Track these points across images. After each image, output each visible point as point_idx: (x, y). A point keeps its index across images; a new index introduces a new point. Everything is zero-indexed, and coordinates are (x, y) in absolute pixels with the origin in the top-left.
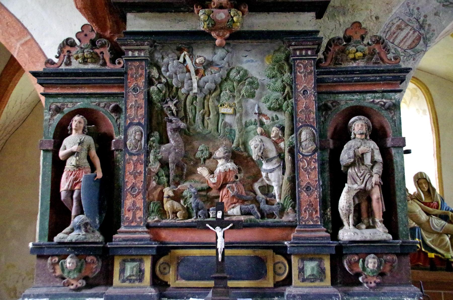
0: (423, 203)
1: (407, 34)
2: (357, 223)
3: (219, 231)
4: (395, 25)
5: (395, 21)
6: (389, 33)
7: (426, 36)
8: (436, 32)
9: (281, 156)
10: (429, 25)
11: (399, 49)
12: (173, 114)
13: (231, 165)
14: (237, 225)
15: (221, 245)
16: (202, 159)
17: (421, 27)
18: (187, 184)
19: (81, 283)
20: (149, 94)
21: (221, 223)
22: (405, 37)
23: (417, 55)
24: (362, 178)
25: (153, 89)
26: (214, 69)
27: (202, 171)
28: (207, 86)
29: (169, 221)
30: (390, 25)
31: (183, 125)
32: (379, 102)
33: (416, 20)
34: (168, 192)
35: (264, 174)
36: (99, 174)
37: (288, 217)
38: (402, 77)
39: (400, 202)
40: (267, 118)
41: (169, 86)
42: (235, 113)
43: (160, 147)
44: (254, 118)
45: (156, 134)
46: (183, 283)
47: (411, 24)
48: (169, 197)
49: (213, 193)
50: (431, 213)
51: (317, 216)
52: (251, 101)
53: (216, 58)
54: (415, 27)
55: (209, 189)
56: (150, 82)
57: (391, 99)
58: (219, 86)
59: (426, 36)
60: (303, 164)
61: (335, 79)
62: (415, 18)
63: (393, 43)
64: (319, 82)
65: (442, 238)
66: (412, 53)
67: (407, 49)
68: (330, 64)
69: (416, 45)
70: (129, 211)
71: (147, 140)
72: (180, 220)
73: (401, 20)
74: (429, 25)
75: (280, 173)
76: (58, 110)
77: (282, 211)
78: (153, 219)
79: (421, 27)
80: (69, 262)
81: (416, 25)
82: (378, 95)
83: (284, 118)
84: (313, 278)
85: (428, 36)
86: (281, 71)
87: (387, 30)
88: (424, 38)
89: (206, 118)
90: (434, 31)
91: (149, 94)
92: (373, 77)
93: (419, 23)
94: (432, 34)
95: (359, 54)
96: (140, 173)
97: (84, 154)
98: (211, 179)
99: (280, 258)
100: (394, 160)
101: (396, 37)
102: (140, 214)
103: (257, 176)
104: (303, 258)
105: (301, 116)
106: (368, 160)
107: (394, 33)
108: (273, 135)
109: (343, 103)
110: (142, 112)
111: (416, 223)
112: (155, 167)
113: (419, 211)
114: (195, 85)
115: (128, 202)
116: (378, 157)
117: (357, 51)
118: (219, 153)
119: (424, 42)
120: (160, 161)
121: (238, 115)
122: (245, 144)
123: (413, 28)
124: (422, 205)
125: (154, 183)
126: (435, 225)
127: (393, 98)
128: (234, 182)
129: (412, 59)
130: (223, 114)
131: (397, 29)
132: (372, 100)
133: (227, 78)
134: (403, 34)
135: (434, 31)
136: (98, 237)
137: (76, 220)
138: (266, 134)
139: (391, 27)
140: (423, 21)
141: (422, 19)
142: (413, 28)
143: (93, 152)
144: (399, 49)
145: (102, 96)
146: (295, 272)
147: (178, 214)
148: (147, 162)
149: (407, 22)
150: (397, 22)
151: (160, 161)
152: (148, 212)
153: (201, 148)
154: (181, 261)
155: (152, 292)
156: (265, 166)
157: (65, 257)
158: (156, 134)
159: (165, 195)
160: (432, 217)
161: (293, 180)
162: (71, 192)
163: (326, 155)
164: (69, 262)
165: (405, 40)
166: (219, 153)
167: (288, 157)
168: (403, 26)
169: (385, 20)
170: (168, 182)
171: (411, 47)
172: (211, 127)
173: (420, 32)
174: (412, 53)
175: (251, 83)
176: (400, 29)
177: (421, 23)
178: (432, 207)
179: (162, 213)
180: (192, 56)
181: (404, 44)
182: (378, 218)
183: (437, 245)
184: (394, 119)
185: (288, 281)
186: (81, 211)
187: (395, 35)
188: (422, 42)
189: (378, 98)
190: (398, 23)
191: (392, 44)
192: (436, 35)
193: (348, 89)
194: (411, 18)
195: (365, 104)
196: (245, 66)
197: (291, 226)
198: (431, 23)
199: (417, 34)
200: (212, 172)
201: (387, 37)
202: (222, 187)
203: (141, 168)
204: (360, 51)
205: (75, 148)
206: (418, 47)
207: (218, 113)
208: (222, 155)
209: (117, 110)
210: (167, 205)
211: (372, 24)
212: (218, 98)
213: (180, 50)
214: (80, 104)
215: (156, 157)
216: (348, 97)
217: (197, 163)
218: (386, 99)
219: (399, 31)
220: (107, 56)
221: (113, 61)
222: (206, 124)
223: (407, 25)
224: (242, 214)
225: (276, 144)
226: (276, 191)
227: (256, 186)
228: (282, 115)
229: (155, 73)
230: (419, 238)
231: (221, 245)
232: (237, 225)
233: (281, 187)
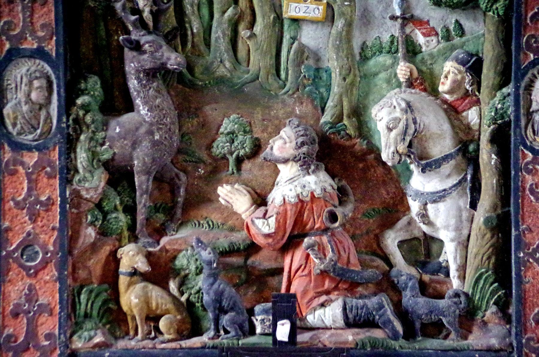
12: (142, 24)
16: (232, 160)
18: (185, 233)
35: (415, 206)
40: (430, 32)
43: (105, 125)
48: (134, 273)
70: (16, 315)
75: (465, 202)
89: (244, 33)
96: (48, 204)
98: (259, 223)
108: (444, 87)
120: (107, 165)
121: (339, 23)
128: (326, 230)
130: (295, 21)
147: (162, 324)
151: (107, 165)
153: (227, 126)
159: (124, 267)
170: (132, 228)
207: (279, 19)
208: (290, 150)
215: (94, 155)
222: (242, 53)
224: (349, 324)
228: (475, 20)
233: (464, 244)
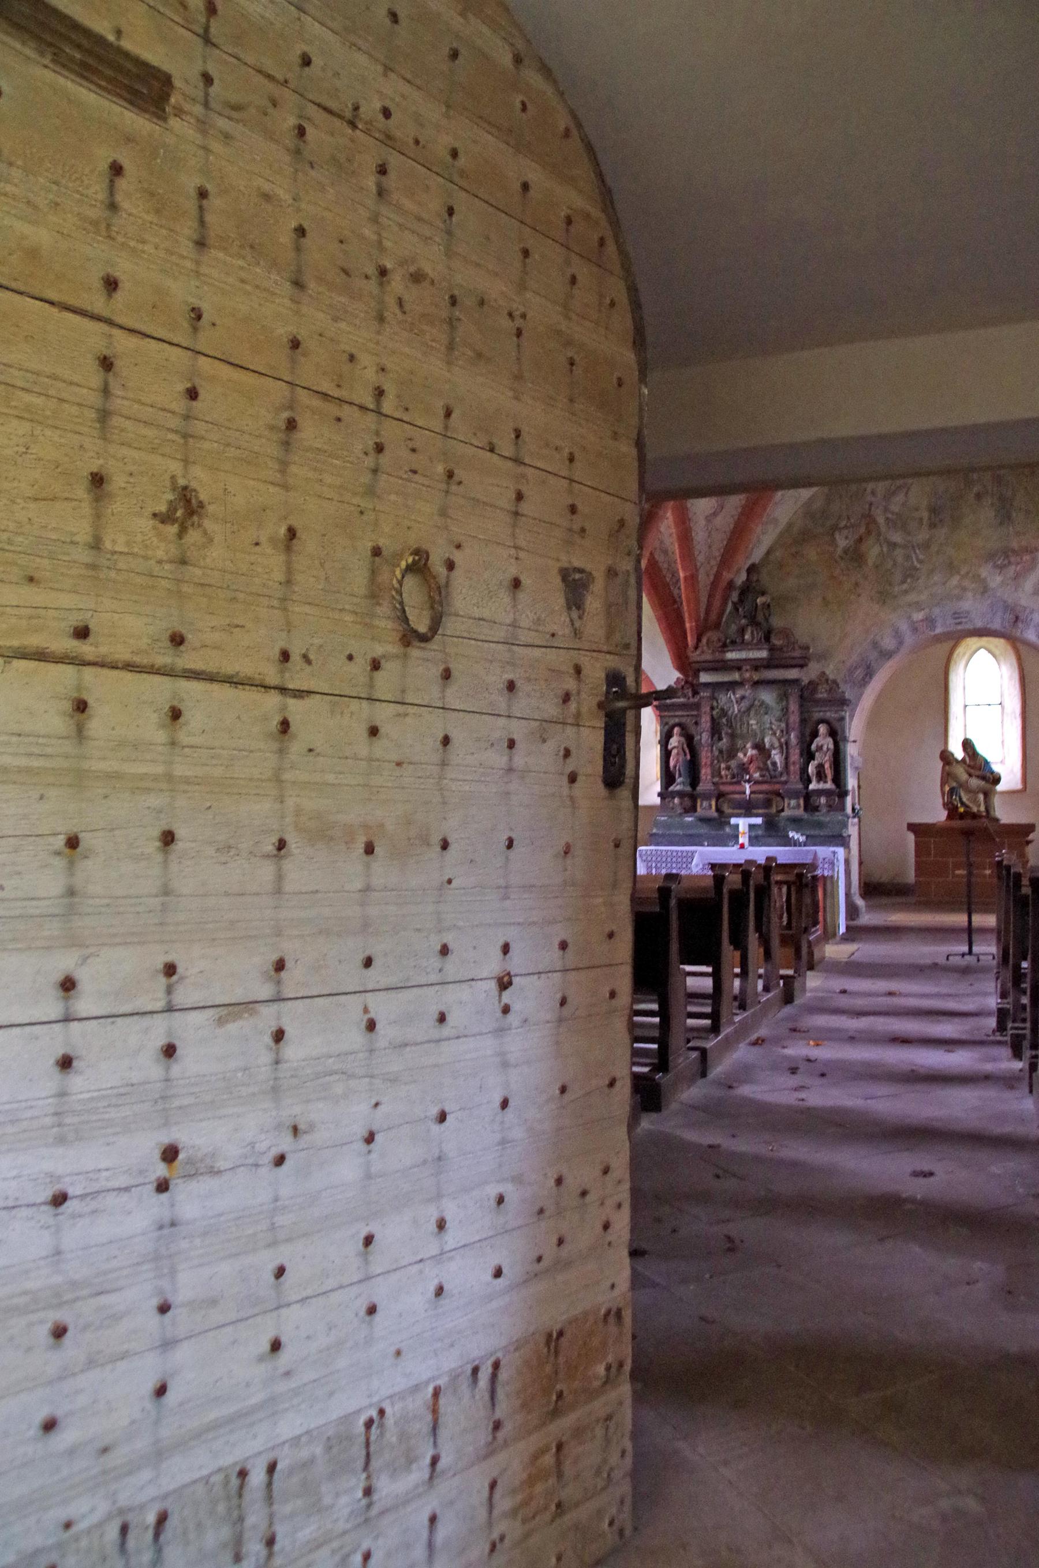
2: (818, 781)
3: (747, 786)
9: (781, 746)
13: (754, 752)
14: (757, 782)
15: (748, 792)
18: (733, 762)
19: (682, 811)
20: (712, 716)
21: (749, 781)
25: (714, 713)
26: (746, 700)
27: (740, 755)
28: (742, 709)
29: (724, 780)
31: (730, 731)
34: (723, 766)
36: (688, 757)
37: (784, 779)
41: (722, 709)
42: (757, 723)
44: (768, 726)
45: (717, 736)
46: (730, 811)
49: (746, 766)
51: (798, 777)
52: (766, 717)
53: (747, 694)
55: (744, 764)
56: (712, 708)
58: (749, 709)
60: (791, 751)
64: (801, 706)
71: (712, 740)
72: (729, 780)
76: (667, 724)
77: (781, 774)
78: (716, 780)
80: (676, 800)
83: (783, 725)
84: (794, 808)
86: (781, 700)
91: (712, 715)
97: (680, 747)
99: (779, 799)
102: (709, 777)
103: (770, 756)
104: (790, 799)
105: (791, 725)
106: (825, 748)
110: (709, 724)
112: (716, 753)
114: (736, 709)
115: (703, 771)
116: (831, 746)
118: (749, 745)
122: (763, 740)
125: (716, 762)
133: (752, 706)
136: (688, 789)
137: (679, 780)
138: (774, 734)
143: (685, 746)
145: (688, 716)
146: (786, 805)
148: (712, 751)
152: (713, 777)
154: (730, 801)
155: (715, 815)
156: (773, 752)
157: (674, 798)
158: (717, 736)
161: (787, 758)
162: (675, 767)
163: (805, 745)
164: (676, 800)
166: (749, 745)
167: (784, 747)
169: (848, 664)
171: (863, 679)
172: (745, 731)
175: (766, 708)
179: (721, 777)
180: (734, 694)
182: (830, 777)
185: (783, 810)
186: (680, 776)
196: (763, 698)
197: (786, 782)
200: (745, 755)
202: (751, 762)
203: (709, 754)
205: (676, 744)
209: (696, 723)
210: (723, 773)
212: (749, 715)
213: (728, 690)
214: (677, 720)
216: (817, 714)
217: (738, 751)
220: (690, 694)
221: (693, 696)
225: (779, 740)
226: (779, 765)
227: (769, 762)
229: (715, 704)
231: (748, 792)
232: (757, 782)
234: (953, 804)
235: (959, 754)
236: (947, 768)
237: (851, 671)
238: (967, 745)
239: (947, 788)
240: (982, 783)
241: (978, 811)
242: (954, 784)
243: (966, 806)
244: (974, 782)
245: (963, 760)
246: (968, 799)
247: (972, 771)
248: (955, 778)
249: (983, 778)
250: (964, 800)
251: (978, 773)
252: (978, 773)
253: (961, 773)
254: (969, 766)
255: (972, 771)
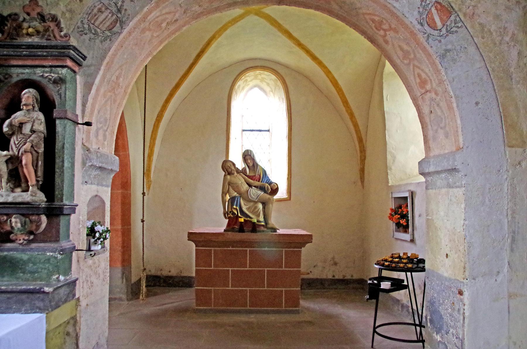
0: (247, 176)
1: (107, 17)
4: (97, 8)
5: (96, 4)
6: (91, 15)
7: (122, 19)
8: (130, 16)
10: (126, 10)
11: (98, 30)
17: (119, 11)
22: (105, 19)
23: (114, 36)
24: (17, 146)
30: (92, 8)
32: (47, 76)
33: (115, 5)
38: (66, 53)
39: (58, 168)
47: (110, 8)
50: (252, 185)
54: (113, 11)
57: (58, 74)
59: (122, 19)
61: (5, 53)
62: (114, 2)
63: (93, 24)
65: (256, 205)
66: (109, 34)
67: (105, 31)
68: (6, 39)
69: (113, 28)
73: (102, 4)
74: (126, 10)
79: (119, 11)
81: (114, 9)
82: (47, 69)
85: (124, 20)
87: (89, 12)
88: (120, 21)
90: (129, 15)
92: (41, 52)
93: (117, 7)
94: (127, 18)
95: (30, 30)
100: (57, 130)
101: (97, 19)
107: (95, 15)
109: (14, 76)
111: (238, 193)
113: (242, 183)
117: (29, 27)
119: (120, 25)
123: (111, 12)
124: (246, 177)
126: (252, 194)
127: (60, 72)
129: (108, 40)
131: (98, 12)
132: (41, 74)
134: (103, 16)
135: (129, 15)
139: (93, 9)
140: (122, 6)
141: (120, 3)
142: (111, 12)
144: (98, 30)
149: (106, 5)
150: (98, 5)
160: (252, 188)
165: (104, 22)
168: (103, 9)
173: (118, 15)
174: (109, 34)
176: (101, 12)
177: (119, 8)
178: (254, 180)
181: (103, 26)
183: (251, 211)
184: (60, 92)
187: (96, 17)
188: (118, 25)
189: (47, 72)
190: (100, 6)
191: (93, 26)
192: (130, 19)
193: (20, 63)
194: (111, 2)
195: (35, 78)
198: (127, 8)
199: (114, 17)
201: (89, 18)
204: (32, 28)
206: (115, 29)
211: (76, 6)
216: (20, 70)
218: (54, 73)
219: (100, 13)
223: (107, 8)
230: (237, 206)
234: (233, 214)
235: (240, 165)
236: (229, 177)
237: (92, 16)
238: (247, 156)
239: (228, 197)
240: (261, 193)
241: (258, 221)
242: (235, 194)
243: (247, 216)
244: (254, 193)
245: (244, 169)
246: (248, 209)
247: (251, 181)
248: (236, 188)
249: (262, 188)
250: (244, 209)
251: (257, 183)
252: (257, 183)
253: (240, 180)
254: (249, 177)
255: (251, 181)
